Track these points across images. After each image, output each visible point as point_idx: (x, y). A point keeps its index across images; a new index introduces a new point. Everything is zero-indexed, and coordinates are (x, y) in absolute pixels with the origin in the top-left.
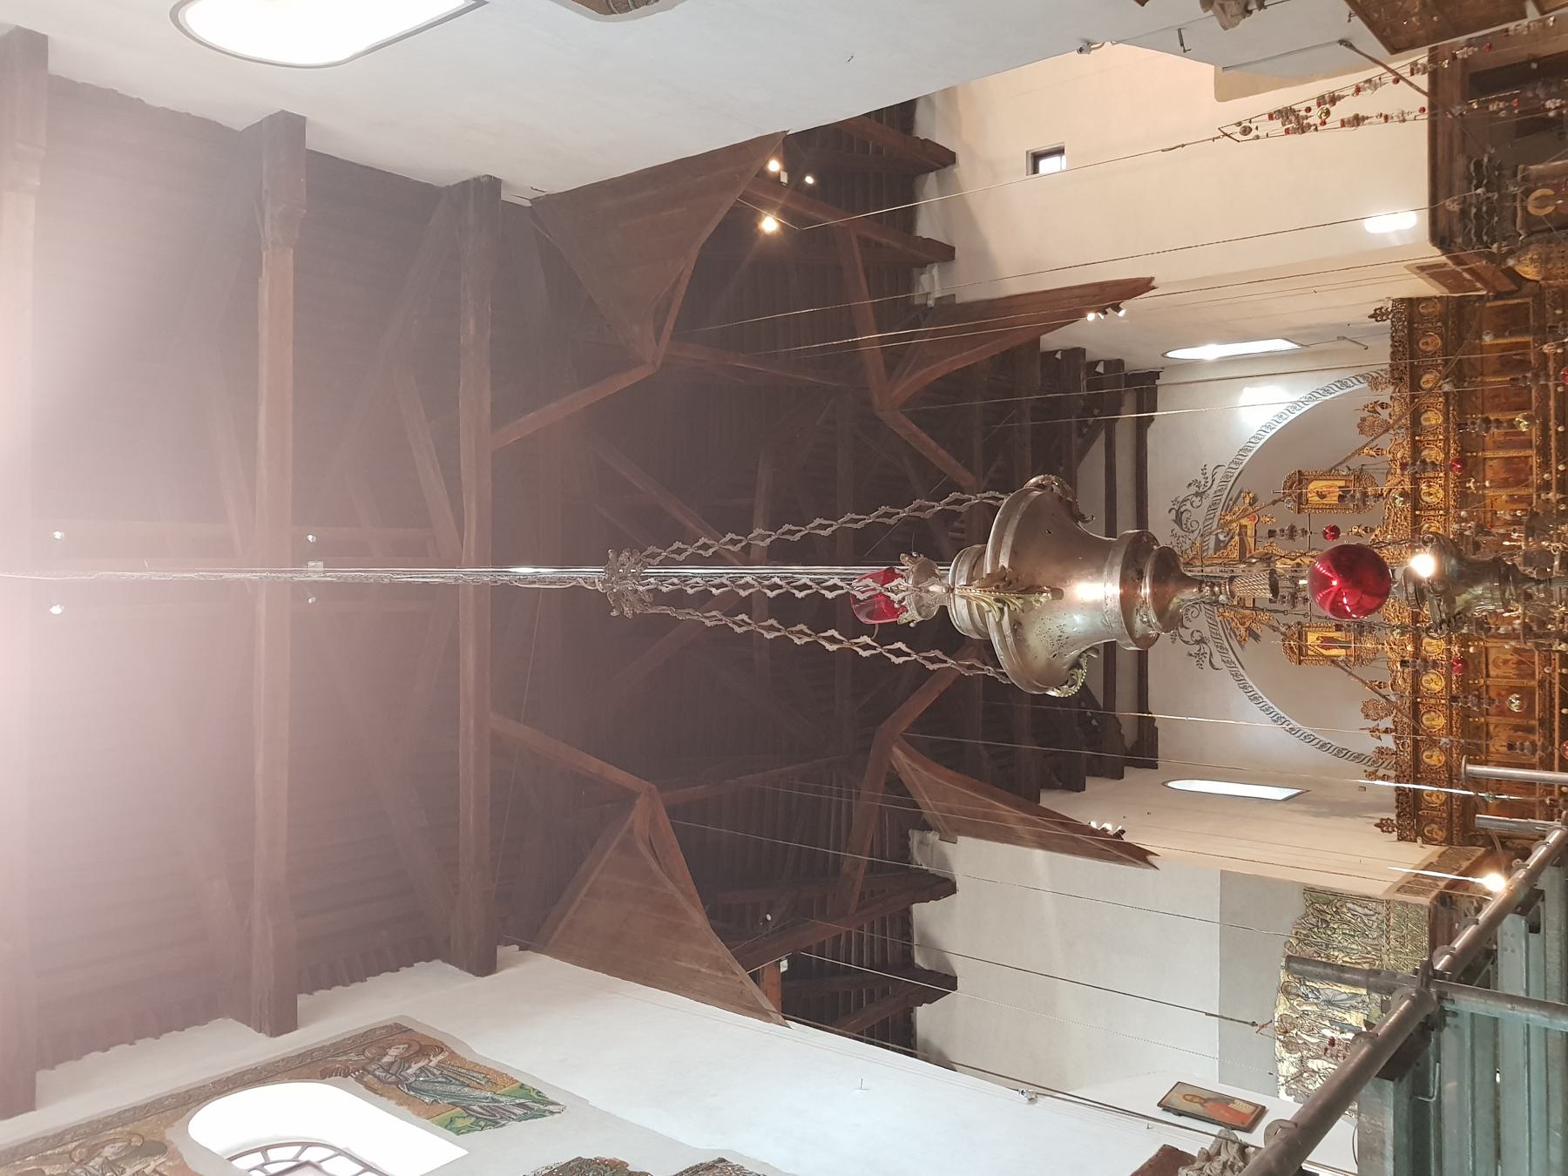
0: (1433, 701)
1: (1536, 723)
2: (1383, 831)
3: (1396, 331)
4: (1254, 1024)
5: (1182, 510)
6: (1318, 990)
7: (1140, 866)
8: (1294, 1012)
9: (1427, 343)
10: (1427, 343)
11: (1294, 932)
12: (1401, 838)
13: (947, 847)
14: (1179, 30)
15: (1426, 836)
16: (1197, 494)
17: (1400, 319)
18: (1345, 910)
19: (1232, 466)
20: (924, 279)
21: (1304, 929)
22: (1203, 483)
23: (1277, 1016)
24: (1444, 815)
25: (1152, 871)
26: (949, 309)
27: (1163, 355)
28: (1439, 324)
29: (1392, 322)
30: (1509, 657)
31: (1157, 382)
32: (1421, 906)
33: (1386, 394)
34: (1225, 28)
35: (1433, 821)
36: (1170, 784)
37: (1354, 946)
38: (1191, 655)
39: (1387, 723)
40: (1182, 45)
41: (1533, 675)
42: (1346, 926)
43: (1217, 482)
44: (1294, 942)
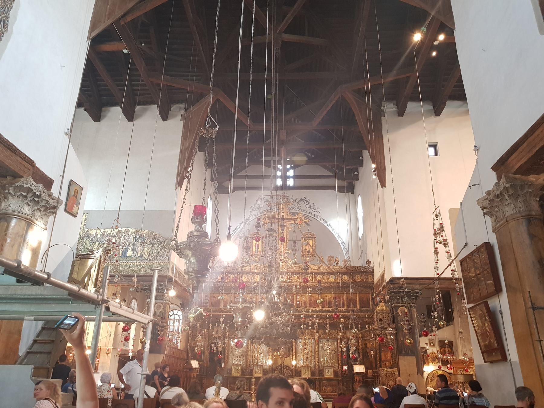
3: (363, 268)
4: (118, 218)
5: (305, 201)
6: (138, 241)
7: (176, 184)
8: (130, 234)
9: (358, 277)
10: (358, 277)
11: (157, 234)
13: (179, 117)
14: (479, 184)
16: (310, 206)
17: (367, 269)
18: (165, 249)
19: (320, 218)
20: (392, 105)
21: (158, 237)
22: (314, 208)
23: (129, 228)
26: (379, 115)
28: (364, 281)
31: (350, 193)
33: (342, 264)
34: (477, 201)
36: (210, 197)
37: (153, 252)
40: (473, 185)
42: (160, 250)
43: (315, 213)
44: (154, 234)
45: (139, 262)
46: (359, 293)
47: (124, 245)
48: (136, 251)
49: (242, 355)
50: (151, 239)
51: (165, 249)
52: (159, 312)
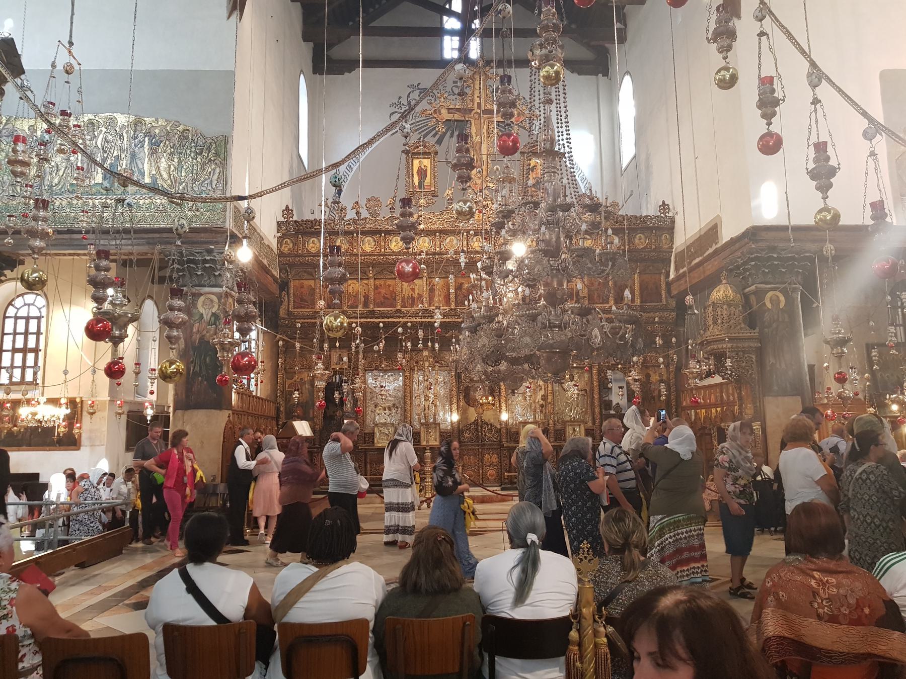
0: (383, 244)
1: (371, 308)
2: (283, 211)
3: (651, 218)
4: (71, 43)
6: (142, 146)
8: (120, 129)
9: (640, 239)
10: (640, 239)
11: (189, 128)
12: (279, 224)
15: (283, 240)
17: (660, 221)
18: (213, 166)
21: (193, 136)
23: (115, 115)
24: (300, 252)
25: (226, 14)
27: (628, 72)
28: (654, 247)
29: (658, 217)
30: (416, 292)
31: (600, 75)
32: (224, 222)
35: (295, 244)
36: (302, 75)
37: (183, 174)
38: (400, 98)
39: (364, 214)
41: (404, 306)
42: (199, 166)
44: (180, 128)
45: (150, 198)
46: (640, 273)
47: (105, 155)
48: (140, 171)
49: (394, 405)
50: (175, 140)
51: (213, 166)
52: (210, 314)
